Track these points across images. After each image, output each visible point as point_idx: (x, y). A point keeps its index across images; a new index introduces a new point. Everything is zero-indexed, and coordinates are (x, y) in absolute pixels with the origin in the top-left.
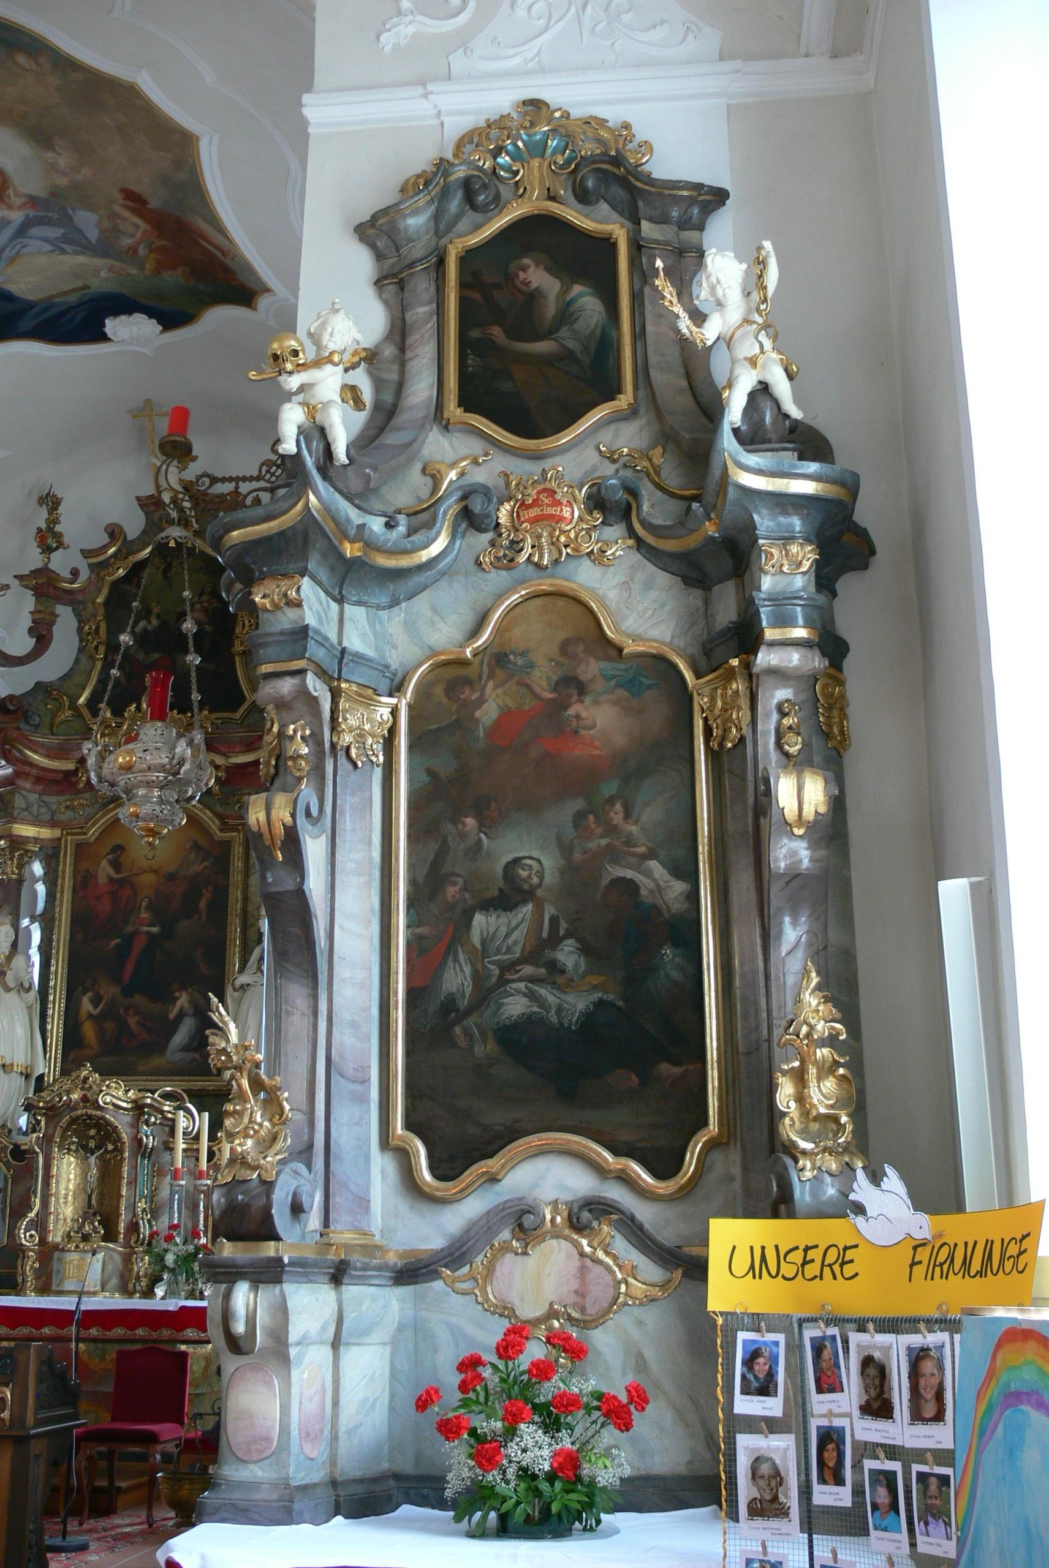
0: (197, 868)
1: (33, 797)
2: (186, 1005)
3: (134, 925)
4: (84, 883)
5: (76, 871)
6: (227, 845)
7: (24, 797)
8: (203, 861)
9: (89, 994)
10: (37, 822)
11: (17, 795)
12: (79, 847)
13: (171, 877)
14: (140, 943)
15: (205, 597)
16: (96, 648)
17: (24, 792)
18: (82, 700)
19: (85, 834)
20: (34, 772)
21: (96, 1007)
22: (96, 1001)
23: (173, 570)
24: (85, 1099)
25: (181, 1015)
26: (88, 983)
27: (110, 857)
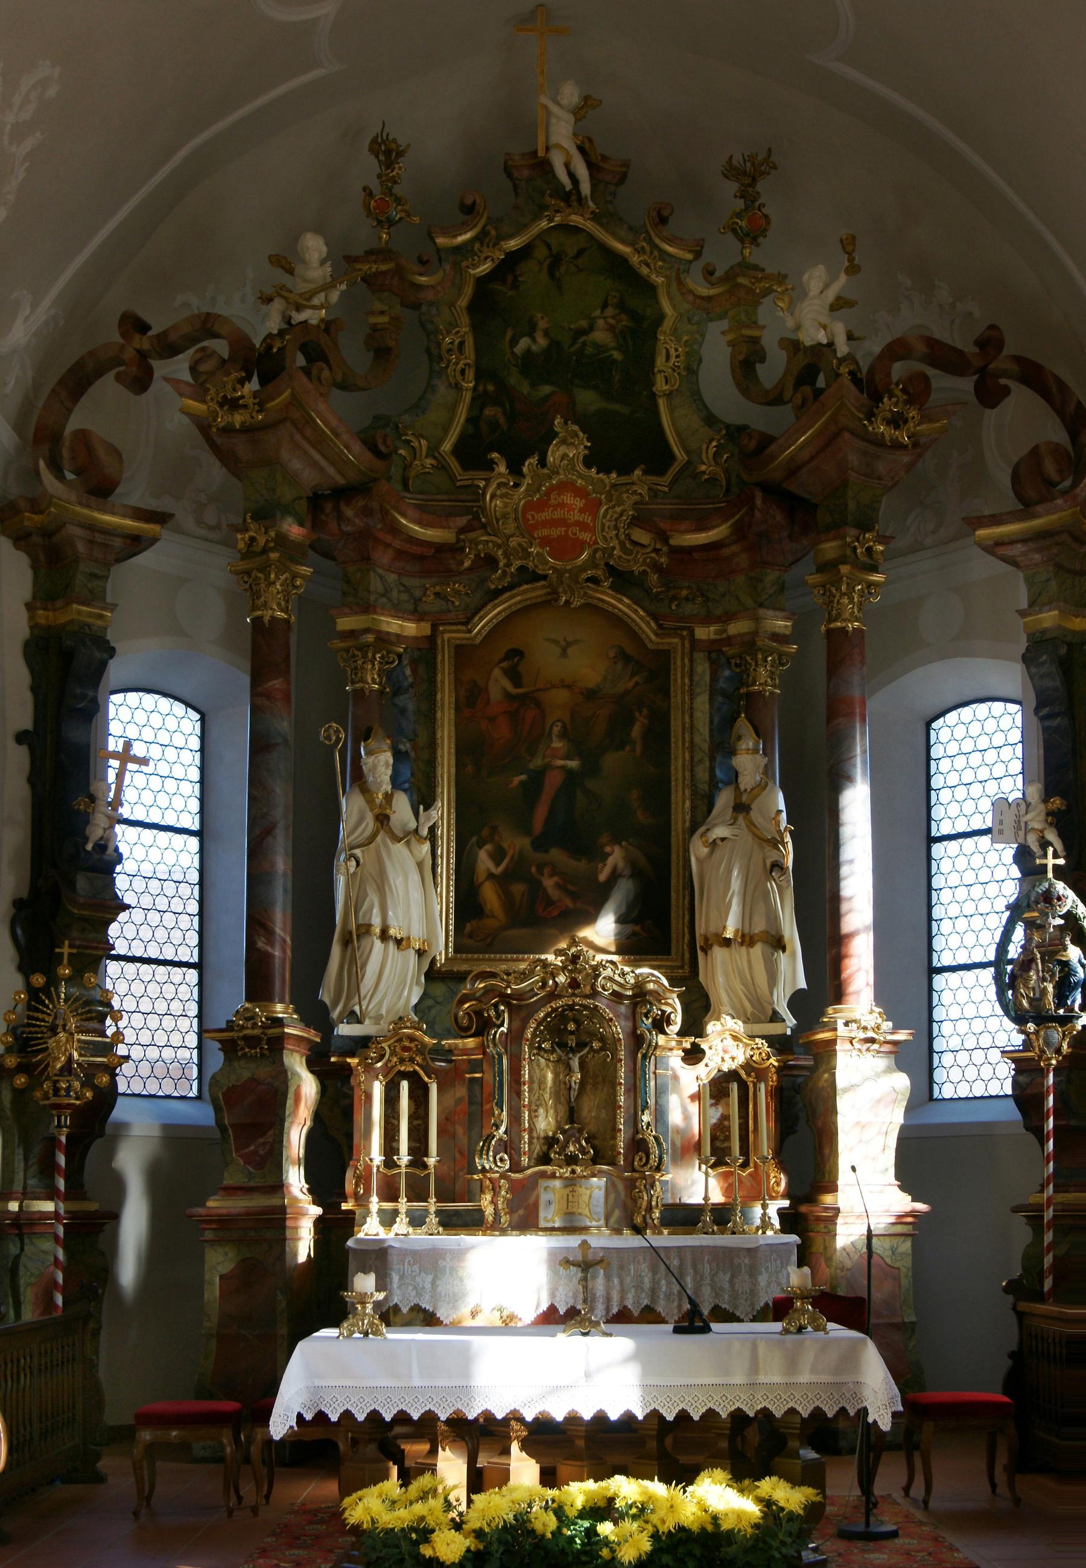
1: (392, 577)
2: (621, 864)
3: (544, 757)
5: (458, 682)
6: (664, 657)
7: (381, 577)
8: (632, 676)
9: (488, 847)
10: (398, 611)
11: (372, 574)
13: (591, 695)
14: (553, 782)
15: (610, 311)
16: (463, 372)
17: (380, 571)
19: (470, 631)
20: (397, 544)
21: (498, 864)
22: (498, 856)
23: (563, 268)
26: (485, 832)
27: (505, 664)
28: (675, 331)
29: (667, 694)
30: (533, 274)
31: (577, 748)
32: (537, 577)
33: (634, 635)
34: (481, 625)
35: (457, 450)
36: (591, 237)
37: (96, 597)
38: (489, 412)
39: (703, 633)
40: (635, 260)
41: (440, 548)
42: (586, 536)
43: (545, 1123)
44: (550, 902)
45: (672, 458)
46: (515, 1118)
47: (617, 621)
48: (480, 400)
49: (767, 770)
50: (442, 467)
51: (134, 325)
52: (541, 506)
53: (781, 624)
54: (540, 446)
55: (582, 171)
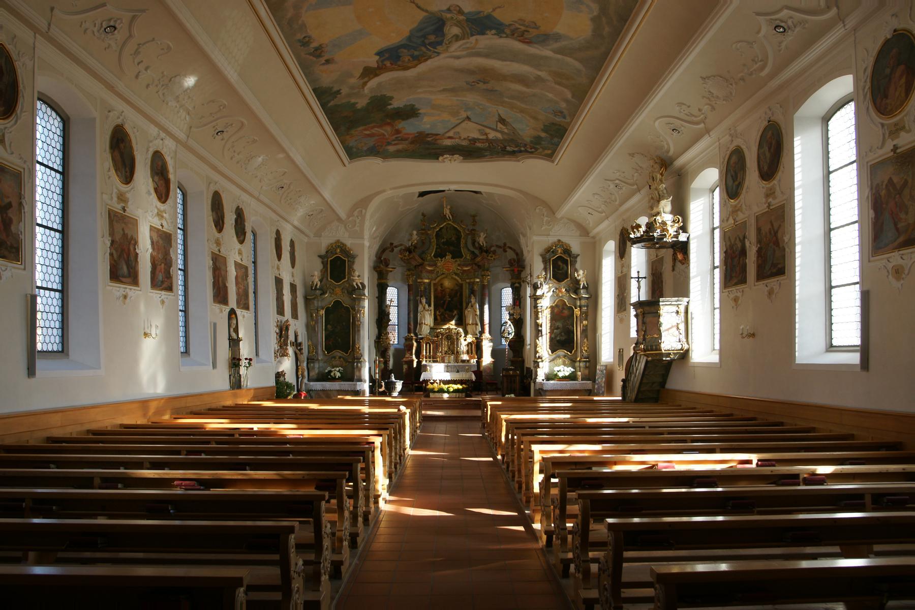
0: (457, 288)
4: (436, 290)
10: (426, 279)
13: (452, 290)
14: (447, 301)
18: (432, 255)
22: (439, 312)
24: (449, 332)
28: (464, 238)
30: (444, 231)
31: (450, 297)
32: (443, 274)
33: (457, 281)
34: (437, 280)
35: (434, 256)
36: (452, 225)
37: (386, 279)
38: (438, 250)
39: (468, 281)
40: (458, 228)
41: (432, 270)
42: (451, 268)
43: (446, 349)
44: (446, 318)
45: (463, 256)
46: (442, 349)
47: (455, 279)
48: (437, 248)
49: (476, 301)
50: (431, 258)
51: (392, 244)
52: (445, 264)
53: (478, 280)
54: (445, 256)
55: (451, 217)
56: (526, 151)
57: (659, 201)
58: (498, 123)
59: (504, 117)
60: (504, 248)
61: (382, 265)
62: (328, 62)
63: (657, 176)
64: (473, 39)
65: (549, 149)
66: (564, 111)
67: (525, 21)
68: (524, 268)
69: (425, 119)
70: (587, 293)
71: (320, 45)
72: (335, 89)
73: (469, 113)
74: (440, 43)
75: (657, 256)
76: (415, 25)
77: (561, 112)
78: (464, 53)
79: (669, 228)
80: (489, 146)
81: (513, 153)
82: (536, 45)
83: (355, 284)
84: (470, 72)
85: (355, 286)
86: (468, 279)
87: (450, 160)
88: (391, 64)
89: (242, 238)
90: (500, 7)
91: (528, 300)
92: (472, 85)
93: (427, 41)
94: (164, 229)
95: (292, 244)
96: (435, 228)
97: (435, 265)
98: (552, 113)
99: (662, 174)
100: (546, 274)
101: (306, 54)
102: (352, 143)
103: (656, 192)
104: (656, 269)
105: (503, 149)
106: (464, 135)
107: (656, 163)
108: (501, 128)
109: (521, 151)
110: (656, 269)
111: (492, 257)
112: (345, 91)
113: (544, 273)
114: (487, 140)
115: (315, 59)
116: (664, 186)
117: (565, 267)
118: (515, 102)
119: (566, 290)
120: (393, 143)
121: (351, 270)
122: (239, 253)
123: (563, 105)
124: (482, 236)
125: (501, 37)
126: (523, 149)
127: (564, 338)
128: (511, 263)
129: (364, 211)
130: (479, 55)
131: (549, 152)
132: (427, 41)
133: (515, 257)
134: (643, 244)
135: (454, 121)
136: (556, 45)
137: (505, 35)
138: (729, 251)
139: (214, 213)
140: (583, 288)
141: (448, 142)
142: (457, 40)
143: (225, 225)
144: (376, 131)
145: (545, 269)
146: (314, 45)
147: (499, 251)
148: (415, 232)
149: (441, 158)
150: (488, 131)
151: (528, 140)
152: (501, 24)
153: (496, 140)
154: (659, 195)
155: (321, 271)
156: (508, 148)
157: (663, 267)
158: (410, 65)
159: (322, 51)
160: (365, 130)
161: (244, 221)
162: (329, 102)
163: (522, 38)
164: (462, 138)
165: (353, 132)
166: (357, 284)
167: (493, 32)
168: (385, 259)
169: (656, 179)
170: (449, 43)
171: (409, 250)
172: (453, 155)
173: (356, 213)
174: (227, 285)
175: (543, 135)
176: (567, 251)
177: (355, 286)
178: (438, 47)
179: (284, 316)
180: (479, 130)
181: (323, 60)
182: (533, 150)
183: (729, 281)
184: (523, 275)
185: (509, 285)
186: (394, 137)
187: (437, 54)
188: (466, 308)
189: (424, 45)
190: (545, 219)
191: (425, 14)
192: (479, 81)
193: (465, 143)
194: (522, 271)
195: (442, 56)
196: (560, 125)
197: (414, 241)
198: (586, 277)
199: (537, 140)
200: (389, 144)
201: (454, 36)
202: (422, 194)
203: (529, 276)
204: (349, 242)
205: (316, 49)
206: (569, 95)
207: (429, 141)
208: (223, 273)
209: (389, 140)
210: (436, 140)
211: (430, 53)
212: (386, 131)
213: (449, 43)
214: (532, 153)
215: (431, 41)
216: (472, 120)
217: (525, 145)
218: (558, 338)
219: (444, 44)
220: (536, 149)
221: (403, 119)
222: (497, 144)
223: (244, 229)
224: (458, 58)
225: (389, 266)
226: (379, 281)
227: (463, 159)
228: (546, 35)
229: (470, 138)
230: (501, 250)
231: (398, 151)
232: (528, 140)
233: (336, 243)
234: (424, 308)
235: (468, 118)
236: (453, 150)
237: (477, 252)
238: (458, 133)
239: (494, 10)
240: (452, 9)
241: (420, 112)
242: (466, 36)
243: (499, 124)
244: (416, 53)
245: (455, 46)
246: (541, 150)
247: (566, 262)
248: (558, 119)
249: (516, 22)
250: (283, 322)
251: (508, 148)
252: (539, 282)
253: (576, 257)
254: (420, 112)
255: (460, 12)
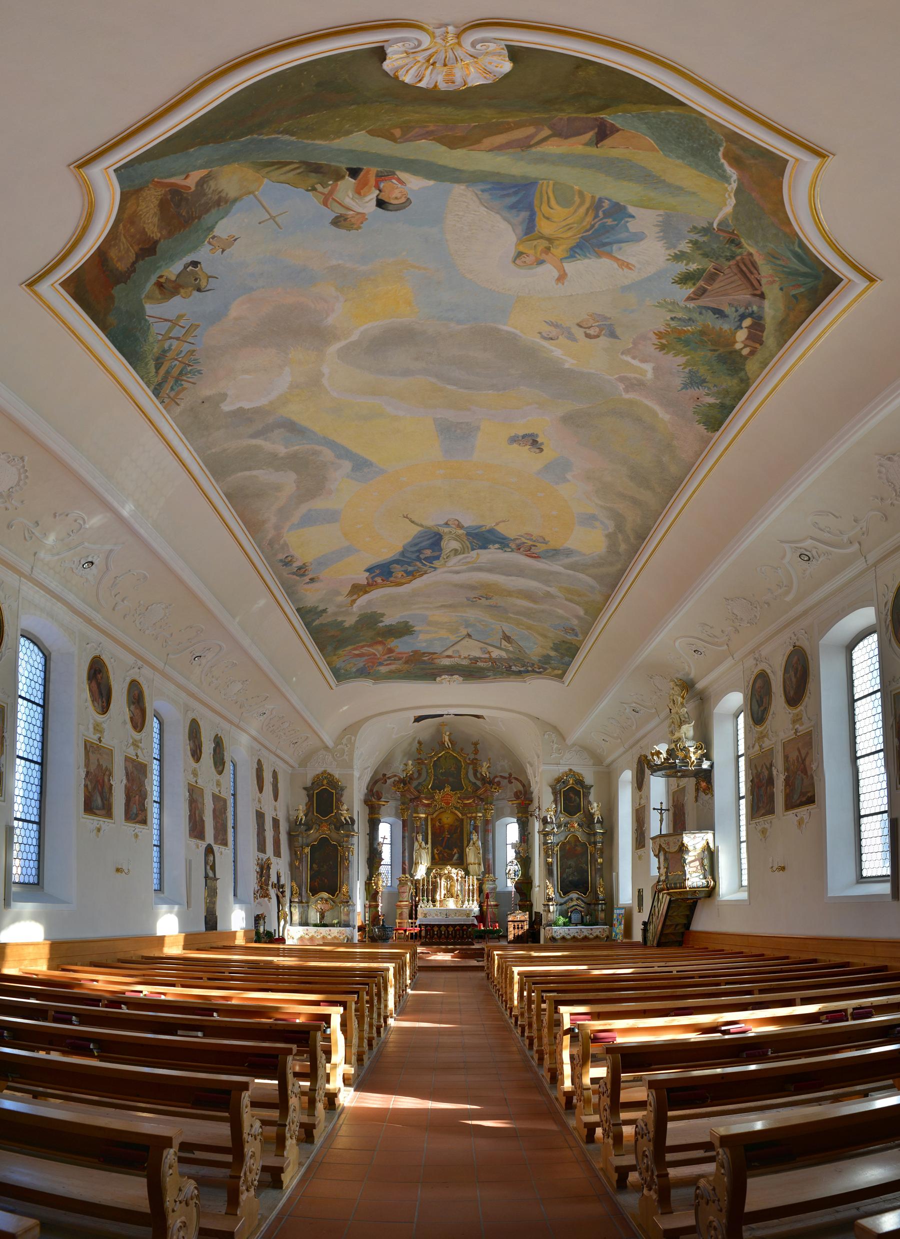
0: (457, 823)
4: (433, 826)
6: (463, 819)
10: (422, 814)
12: (432, 819)
13: (451, 825)
14: (446, 839)
22: (437, 850)
25: (455, 853)
29: (463, 825)
32: (442, 808)
34: (434, 815)
37: (378, 814)
39: (469, 815)
48: (434, 780)
49: (478, 838)
51: (384, 775)
52: (444, 797)
53: (480, 815)
55: (450, 745)
56: (533, 671)
57: (680, 727)
58: (503, 640)
59: (508, 635)
60: (510, 779)
61: (374, 798)
62: (312, 580)
63: (677, 699)
64: (474, 553)
65: (559, 669)
66: (576, 628)
67: (532, 536)
68: (532, 801)
69: (421, 637)
70: (602, 828)
71: (304, 564)
72: (320, 608)
73: (470, 630)
74: (437, 558)
75: (678, 786)
76: (409, 540)
77: (573, 630)
78: (465, 567)
79: (692, 755)
80: (493, 666)
81: (519, 673)
82: (544, 560)
83: (343, 818)
84: (472, 588)
85: (344, 820)
86: (469, 813)
87: (449, 681)
88: (382, 580)
89: (220, 769)
90: (504, 521)
91: (537, 836)
92: (472, 601)
93: (422, 556)
94: (139, 759)
95: (275, 775)
96: (432, 757)
97: (433, 798)
98: (563, 631)
99: (683, 697)
100: (556, 807)
101: (288, 574)
102: (339, 663)
103: (677, 716)
104: (678, 801)
105: (508, 669)
106: (464, 654)
107: (677, 685)
108: (505, 646)
109: (528, 671)
110: (678, 801)
111: (495, 789)
112: (330, 611)
113: (554, 806)
114: (490, 659)
115: (298, 578)
116: (686, 710)
117: (578, 799)
118: (521, 618)
119: (578, 825)
120: (385, 663)
121: (339, 801)
122: (217, 785)
123: (575, 622)
124: (484, 765)
125: (505, 551)
126: (530, 669)
127: (577, 878)
128: (517, 795)
129: (353, 738)
130: (480, 569)
131: (560, 672)
132: (422, 556)
133: (521, 788)
134: (663, 772)
135: (453, 638)
136: (567, 561)
137: (510, 550)
138: (755, 779)
139: (191, 741)
140: (597, 822)
141: (446, 662)
142: (455, 555)
143: (202, 755)
144: (366, 650)
145: (555, 801)
146: (297, 564)
147: (504, 782)
148: (410, 762)
149: (438, 679)
150: (491, 649)
151: (535, 659)
152: (505, 538)
153: (501, 659)
154: (681, 720)
155: (306, 805)
156: (514, 668)
157: (686, 798)
158: (403, 581)
159: (306, 570)
160: (355, 649)
161: (223, 751)
162: (314, 620)
163: (529, 552)
164: (462, 657)
165: (340, 652)
166: (345, 819)
167: (497, 546)
168: (377, 792)
169: (678, 703)
170: (447, 558)
171: (403, 781)
172: (452, 675)
173: (344, 741)
174: (204, 818)
175: (553, 653)
176: (580, 782)
177: (344, 820)
178: (434, 562)
179: (265, 853)
180: (481, 648)
181: (307, 579)
182: (541, 670)
183: (757, 812)
184: (531, 808)
185: (515, 820)
186: (386, 657)
187: (433, 569)
188: (468, 846)
189: (419, 559)
190: (555, 746)
191: (420, 529)
192: (482, 597)
193: (465, 662)
194: (530, 804)
195: (439, 571)
196: (572, 643)
197: (409, 771)
198: (601, 810)
199: (546, 660)
200: (381, 664)
201: (452, 550)
202: (418, 719)
203: (537, 810)
204: (337, 773)
205: (300, 568)
206: (581, 612)
207: (424, 661)
208: (200, 806)
209: (380, 660)
210: (433, 659)
211: (425, 568)
212: (378, 650)
213: (447, 558)
214: (540, 673)
215: (427, 555)
216: (473, 637)
217: (533, 664)
218: (570, 879)
219: (441, 558)
220: (545, 669)
221: (396, 638)
222: (502, 664)
223: (223, 759)
224: (457, 572)
225: (382, 800)
226: (370, 816)
227: (463, 680)
228: (555, 550)
229: (471, 657)
230: (506, 781)
231: (391, 672)
232: (535, 659)
233: (322, 773)
234: (420, 846)
235: (469, 636)
236: (452, 671)
237: (479, 783)
238: (458, 651)
239: (497, 524)
240: (449, 523)
241: (415, 629)
242: (466, 550)
243: (503, 641)
244: (410, 569)
245: (454, 560)
246: (550, 670)
247: (578, 793)
248: (569, 637)
249: (522, 536)
250: (264, 860)
251: (514, 668)
252: (549, 816)
253: (590, 788)
254: (415, 629)
255: (460, 526)
